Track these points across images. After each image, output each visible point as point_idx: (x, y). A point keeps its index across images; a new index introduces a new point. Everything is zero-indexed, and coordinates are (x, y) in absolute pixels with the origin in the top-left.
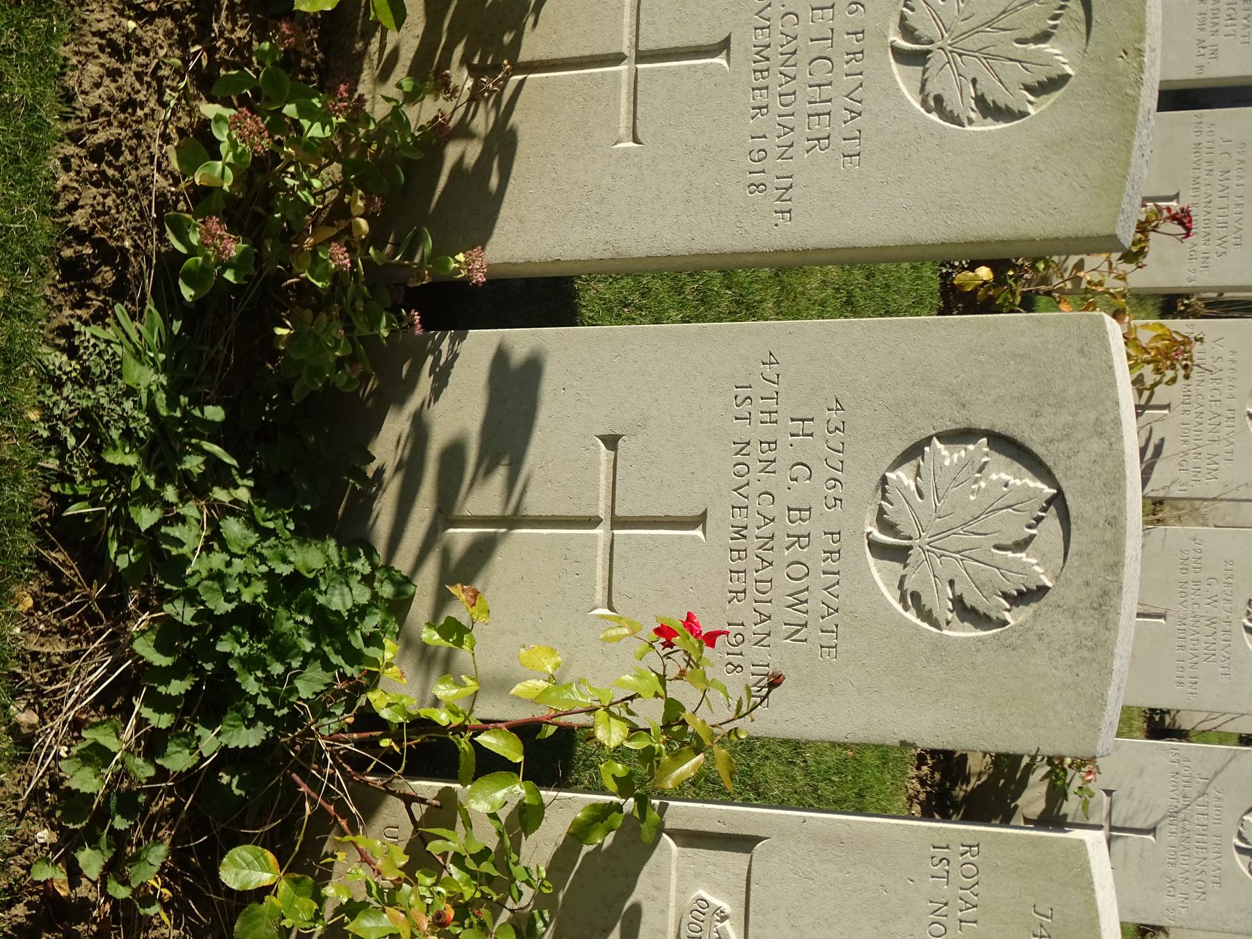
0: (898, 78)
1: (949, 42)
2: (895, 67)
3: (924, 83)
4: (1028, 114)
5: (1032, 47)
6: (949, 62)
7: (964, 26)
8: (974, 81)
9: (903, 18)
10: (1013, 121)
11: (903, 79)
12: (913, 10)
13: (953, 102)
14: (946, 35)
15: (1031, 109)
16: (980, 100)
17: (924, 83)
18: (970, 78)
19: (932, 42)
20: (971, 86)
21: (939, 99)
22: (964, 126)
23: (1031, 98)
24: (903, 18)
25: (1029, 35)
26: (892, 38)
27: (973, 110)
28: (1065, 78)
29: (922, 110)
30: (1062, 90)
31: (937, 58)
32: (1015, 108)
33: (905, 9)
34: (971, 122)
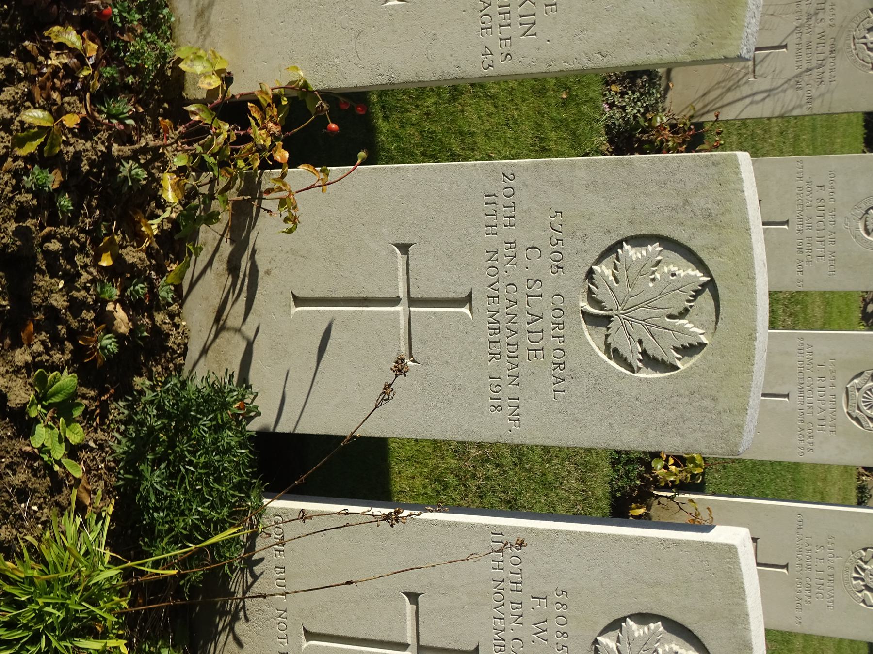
0: (589, 337)
1: (622, 312)
4: (679, 368)
7: (632, 301)
9: (590, 291)
10: (665, 372)
12: (597, 288)
13: (625, 351)
14: (620, 308)
15: (679, 364)
16: (644, 353)
18: (637, 338)
19: (611, 310)
21: (616, 350)
23: (679, 356)
24: (590, 291)
26: (582, 304)
27: (640, 361)
29: (605, 357)
30: (701, 354)
33: (591, 286)
34: (639, 368)
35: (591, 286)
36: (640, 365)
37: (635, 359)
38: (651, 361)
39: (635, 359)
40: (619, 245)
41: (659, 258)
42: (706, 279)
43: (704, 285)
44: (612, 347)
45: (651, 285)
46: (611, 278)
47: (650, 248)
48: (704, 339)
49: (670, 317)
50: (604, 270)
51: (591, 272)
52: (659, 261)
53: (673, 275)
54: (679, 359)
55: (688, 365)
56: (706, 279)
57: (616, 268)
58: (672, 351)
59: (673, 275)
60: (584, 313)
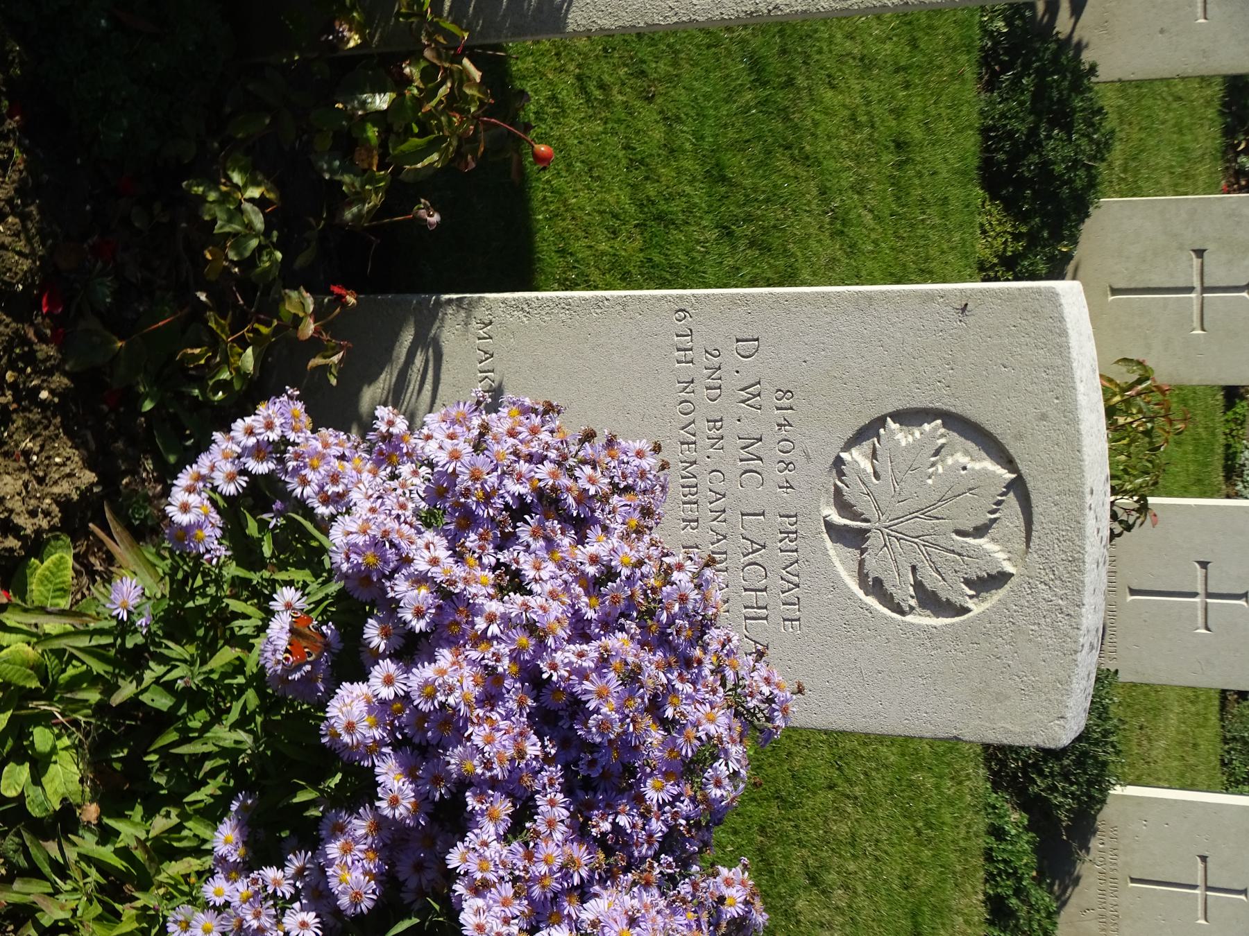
2: (829, 543)
3: (861, 563)
5: (970, 540)
6: (885, 545)
7: (901, 507)
8: (914, 569)
9: (838, 492)
10: (953, 617)
11: (840, 560)
15: (970, 604)
16: (918, 586)
17: (861, 563)
20: (910, 572)
21: (878, 582)
22: (903, 613)
23: (972, 593)
24: (838, 492)
25: (968, 527)
26: (825, 512)
28: (1001, 578)
29: (860, 593)
31: (875, 540)
32: (957, 600)
33: (839, 484)
34: (912, 608)
35: (839, 484)
36: (913, 602)
37: (906, 595)
38: (931, 601)
39: (906, 595)
40: (881, 421)
41: (943, 441)
42: (1013, 476)
43: (1010, 486)
44: (871, 575)
45: (930, 482)
46: (870, 470)
47: (927, 427)
48: (1009, 568)
49: (960, 533)
50: (858, 458)
51: (839, 462)
52: (942, 446)
53: (964, 468)
54: (971, 597)
55: (986, 605)
56: (1013, 476)
57: (874, 455)
58: (963, 586)
59: (964, 468)
60: (829, 526)
